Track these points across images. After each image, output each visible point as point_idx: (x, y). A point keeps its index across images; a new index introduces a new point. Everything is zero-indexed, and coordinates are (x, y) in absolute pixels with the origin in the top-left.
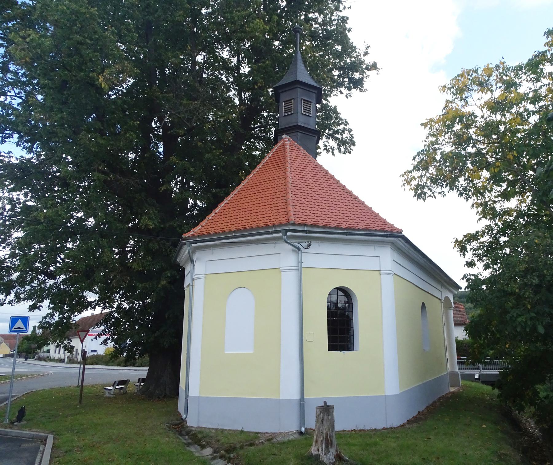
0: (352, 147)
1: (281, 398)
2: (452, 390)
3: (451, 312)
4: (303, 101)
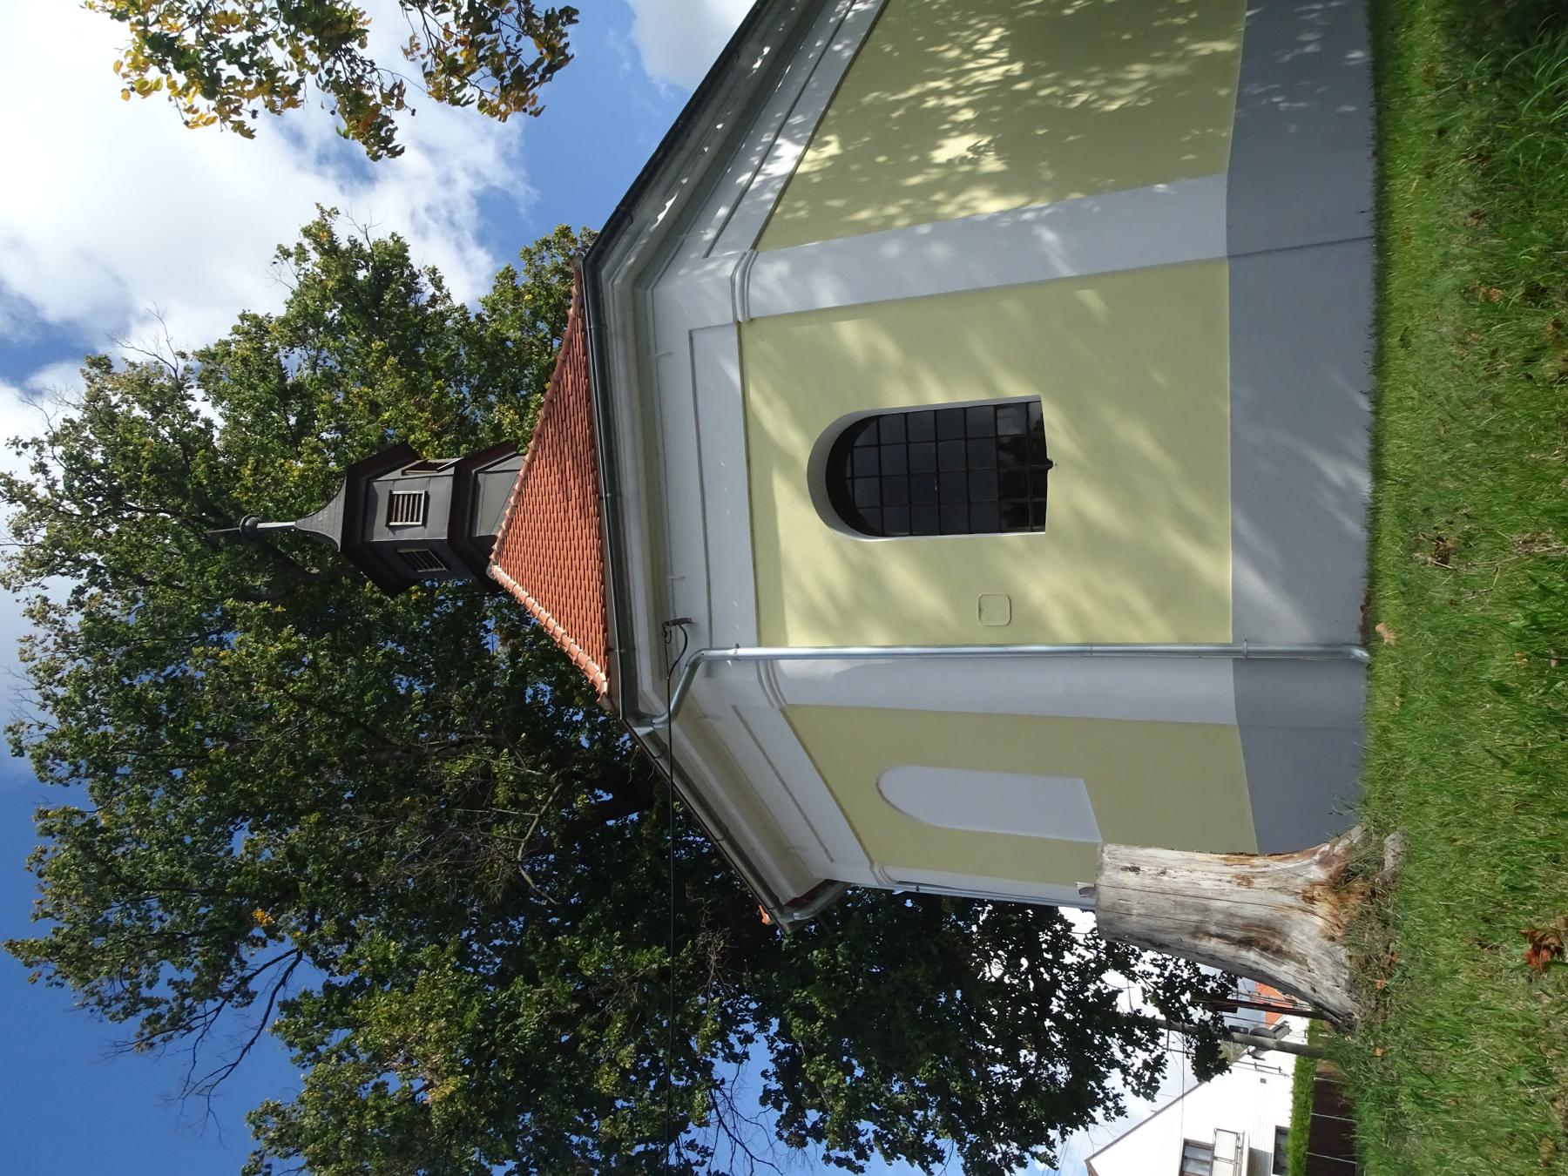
0: (575, 234)
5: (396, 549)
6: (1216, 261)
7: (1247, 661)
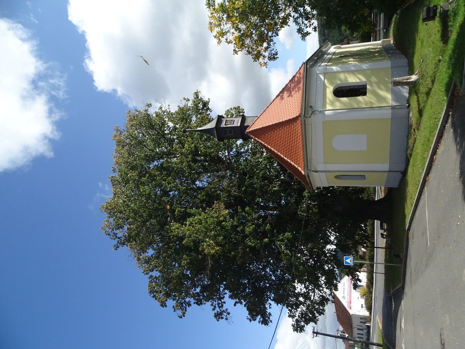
2: (392, 42)
3: (343, 46)
6: (389, 68)
7: (393, 108)
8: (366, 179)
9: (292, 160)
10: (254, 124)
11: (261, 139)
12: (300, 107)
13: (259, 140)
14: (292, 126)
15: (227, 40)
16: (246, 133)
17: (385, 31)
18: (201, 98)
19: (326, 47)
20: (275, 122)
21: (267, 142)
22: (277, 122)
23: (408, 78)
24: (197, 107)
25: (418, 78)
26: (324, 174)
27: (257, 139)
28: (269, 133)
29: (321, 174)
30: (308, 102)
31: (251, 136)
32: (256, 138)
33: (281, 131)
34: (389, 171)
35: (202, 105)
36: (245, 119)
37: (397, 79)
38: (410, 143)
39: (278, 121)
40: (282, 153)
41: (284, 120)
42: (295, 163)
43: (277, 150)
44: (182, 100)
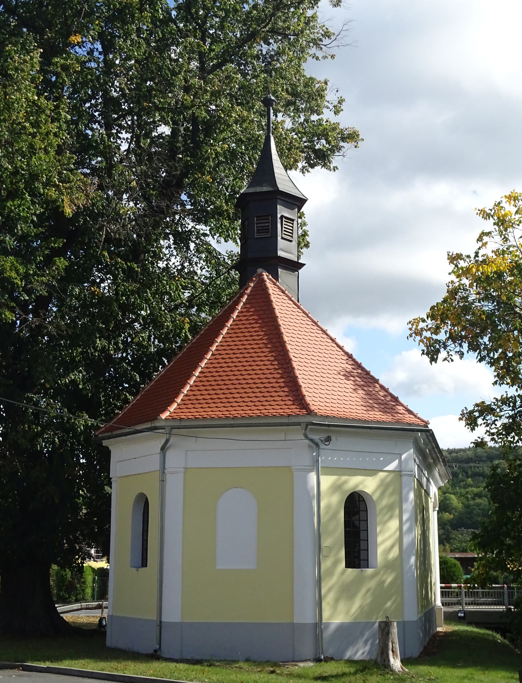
1: (295, 621)
2: (439, 629)
4: (284, 219)
5: (272, 215)
8: (134, 569)
9: (195, 388)
10: (281, 294)
11: (245, 310)
12: (329, 413)
13: (242, 304)
14: (283, 391)
15: (488, 234)
16: (259, 270)
17: (459, 615)
18: (339, 149)
19: (440, 475)
20: (290, 350)
21: (236, 325)
22: (291, 355)
23: (396, 652)
24: (320, 135)
25: (397, 670)
26: (157, 466)
27: (244, 301)
28: (263, 333)
29: (157, 458)
30: (338, 432)
31: (252, 285)
32: (246, 297)
33: (269, 363)
34: (161, 622)
35: (321, 147)
36: (294, 271)
37: (395, 630)
38: (237, 665)
39: (293, 359)
40: (211, 363)
41: (297, 373)
42: (186, 395)
43: (217, 350)
44: (339, 95)
